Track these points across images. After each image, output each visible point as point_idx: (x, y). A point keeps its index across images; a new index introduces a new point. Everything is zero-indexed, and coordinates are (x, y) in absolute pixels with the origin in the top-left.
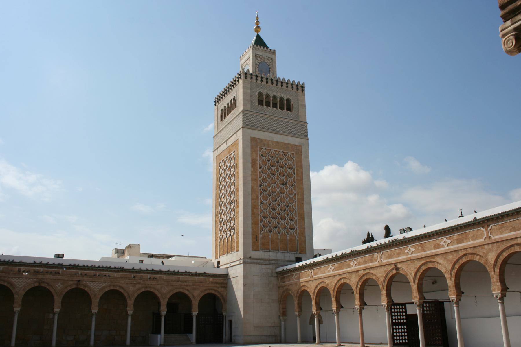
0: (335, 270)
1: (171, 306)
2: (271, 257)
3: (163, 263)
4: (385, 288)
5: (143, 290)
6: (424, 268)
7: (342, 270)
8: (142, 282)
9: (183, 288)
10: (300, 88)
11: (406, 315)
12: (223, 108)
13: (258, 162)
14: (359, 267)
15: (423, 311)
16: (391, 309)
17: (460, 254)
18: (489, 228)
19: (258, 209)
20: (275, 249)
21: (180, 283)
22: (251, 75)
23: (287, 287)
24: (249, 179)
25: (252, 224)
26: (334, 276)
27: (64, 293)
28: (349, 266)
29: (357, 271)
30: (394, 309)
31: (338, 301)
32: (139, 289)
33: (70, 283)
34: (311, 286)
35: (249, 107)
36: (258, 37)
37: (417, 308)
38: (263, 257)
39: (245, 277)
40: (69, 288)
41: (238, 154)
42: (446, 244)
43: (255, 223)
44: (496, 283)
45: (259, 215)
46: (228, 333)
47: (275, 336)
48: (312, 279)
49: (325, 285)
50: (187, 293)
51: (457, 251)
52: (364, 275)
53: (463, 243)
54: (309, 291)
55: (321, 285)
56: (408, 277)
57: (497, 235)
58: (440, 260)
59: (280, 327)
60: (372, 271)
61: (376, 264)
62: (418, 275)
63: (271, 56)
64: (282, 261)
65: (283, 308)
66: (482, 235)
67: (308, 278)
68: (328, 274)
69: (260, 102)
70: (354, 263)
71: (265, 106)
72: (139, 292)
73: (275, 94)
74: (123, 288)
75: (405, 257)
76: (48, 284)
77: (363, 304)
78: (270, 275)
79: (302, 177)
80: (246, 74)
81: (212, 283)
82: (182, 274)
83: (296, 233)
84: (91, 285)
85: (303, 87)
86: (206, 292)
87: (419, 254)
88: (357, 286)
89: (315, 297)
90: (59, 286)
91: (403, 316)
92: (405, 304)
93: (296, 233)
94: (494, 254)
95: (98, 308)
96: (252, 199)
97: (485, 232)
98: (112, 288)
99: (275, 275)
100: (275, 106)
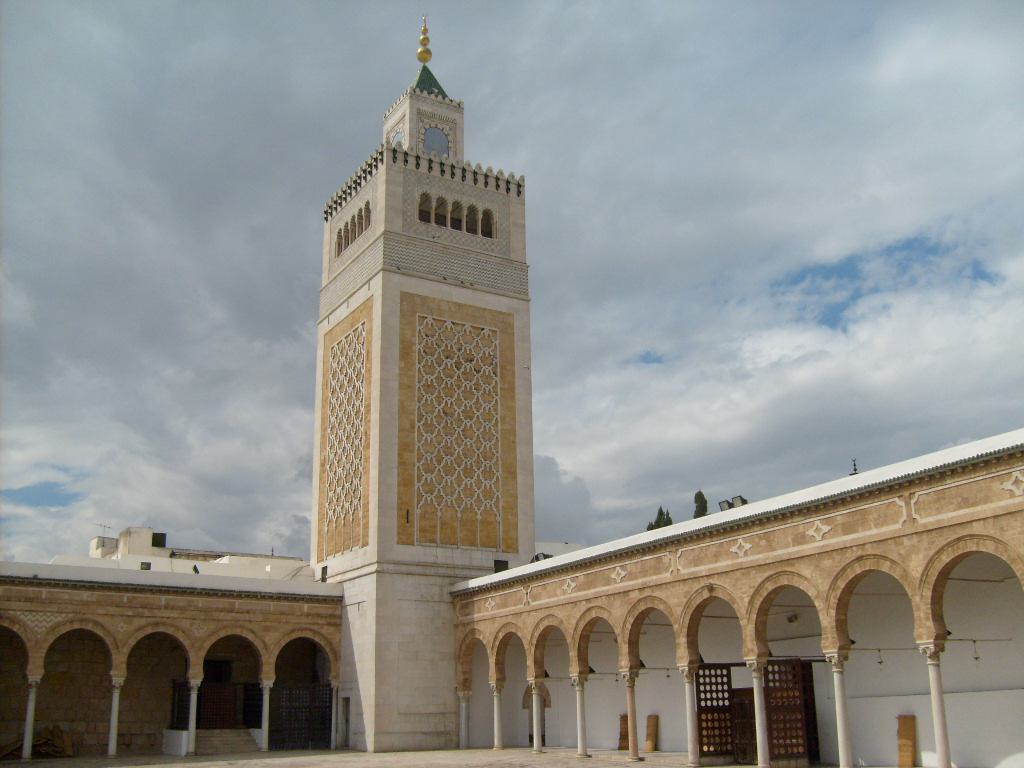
0: (578, 588)
1: (216, 667)
2: (441, 560)
3: (195, 569)
4: (685, 630)
5: (149, 631)
6: (770, 587)
7: (593, 591)
8: (146, 612)
9: (241, 627)
10: (513, 188)
11: (731, 691)
13: (416, 348)
14: (631, 583)
15: (767, 681)
16: (698, 676)
17: (850, 556)
18: (913, 501)
19: (412, 452)
20: (450, 542)
21: (234, 614)
22: (406, 154)
24: (396, 385)
25: (399, 485)
26: (575, 603)
28: (608, 581)
29: (626, 593)
30: (704, 676)
31: (583, 658)
32: (140, 628)
34: (524, 623)
35: (398, 226)
36: (426, 72)
37: (754, 674)
38: (423, 559)
39: (381, 602)
42: (819, 534)
43: (405, 483)
44: (924, 622)
45: (414, 466)
46: (341, 727)
47: (446, 733)
48: (528, 609)
49: (555, 623)
50: (250, 637)
51: (843, 549)
52: (640, 600)
53: (857, 531)
54: (520, 635)
55: (546, 623)
56: (735, 606)
57: (930, 515)
58: (806, 570)
59: (457, 714)
60: (657, 594)
61: (666, 576)
62: (757, 604)
63: (453, 115)
64: (464, 568)
65: (464, 673)
66: (898, 514)
67: (520, 607)
68: (562, 598)
69: (424, 216)
70: (619, 574)
71: (433, 224)
72: (141, 635)
73: (458, 197)
74: (102, 626)
75: (729, 562)
77: (637, 665)
78: (436, 598)
79: (514, 382)
80: (395, 151)
81: (308, 615)
82: (240, 595)
83: (497, 507)
84: (28, 619)
85: (519, 186)
86: (294, 636)
87: (760, 556)
88: (624, 625)
89: (533, 650)
91: (723, 691)
92: (728, 666)
93: (497, 507)
94: (921, 556)
95: (42, 671)
96: (401, 430)
97: (904, 510)
98: (76, 626)
99: (447, 598)
100: (456, 224)
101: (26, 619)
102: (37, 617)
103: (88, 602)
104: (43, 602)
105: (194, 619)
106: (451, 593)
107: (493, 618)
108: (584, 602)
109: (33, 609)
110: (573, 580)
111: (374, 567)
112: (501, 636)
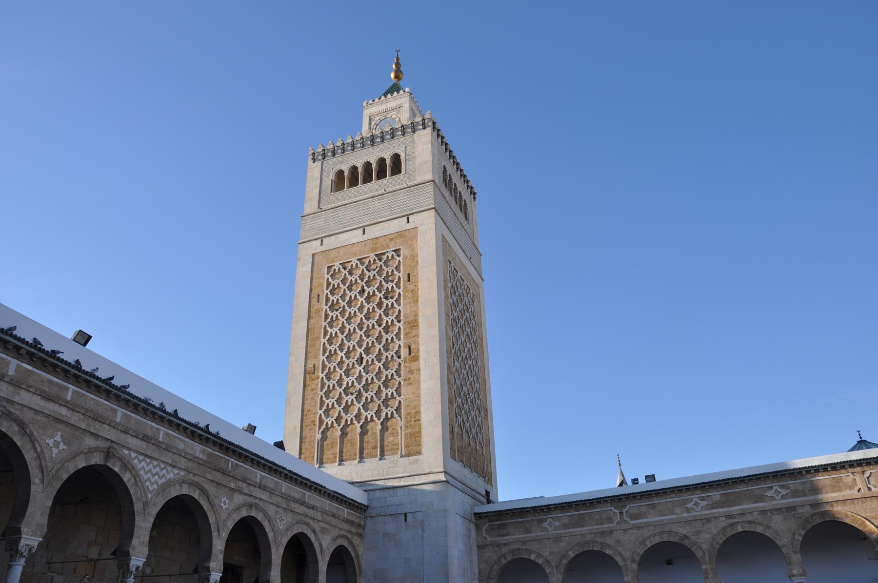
7: (737, 508)
9: (308, 524)
12: (346, 169)
23: (516, 547)
27: (65, 477)
28: (761, 498)
29: (791, 509)
33: (90, 442)
34: (618, 541)
40: (81, 463)
41: (414, 257)
48: (624, 526)
49: (675, 539)
50: (312, 537)
52: (814, 515)
54: (608, 552)
76: (22, 425)
81: (347, 521)
84: (141, 465)
90: (57, 444)
95: (146, 550)
101: (139, 466)
102: (151, 466)
103: (198, 458)
104: (158, 445)
105: (278, 507)
106: (475, 514)
107: (557, 539)
108: (724, 519)
109: (149, 453)
110: (703, 499)
111: (442, 477)
112: (571, 554)
